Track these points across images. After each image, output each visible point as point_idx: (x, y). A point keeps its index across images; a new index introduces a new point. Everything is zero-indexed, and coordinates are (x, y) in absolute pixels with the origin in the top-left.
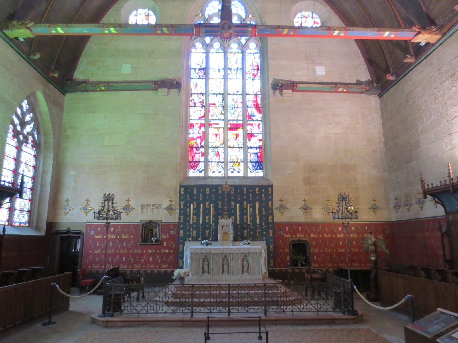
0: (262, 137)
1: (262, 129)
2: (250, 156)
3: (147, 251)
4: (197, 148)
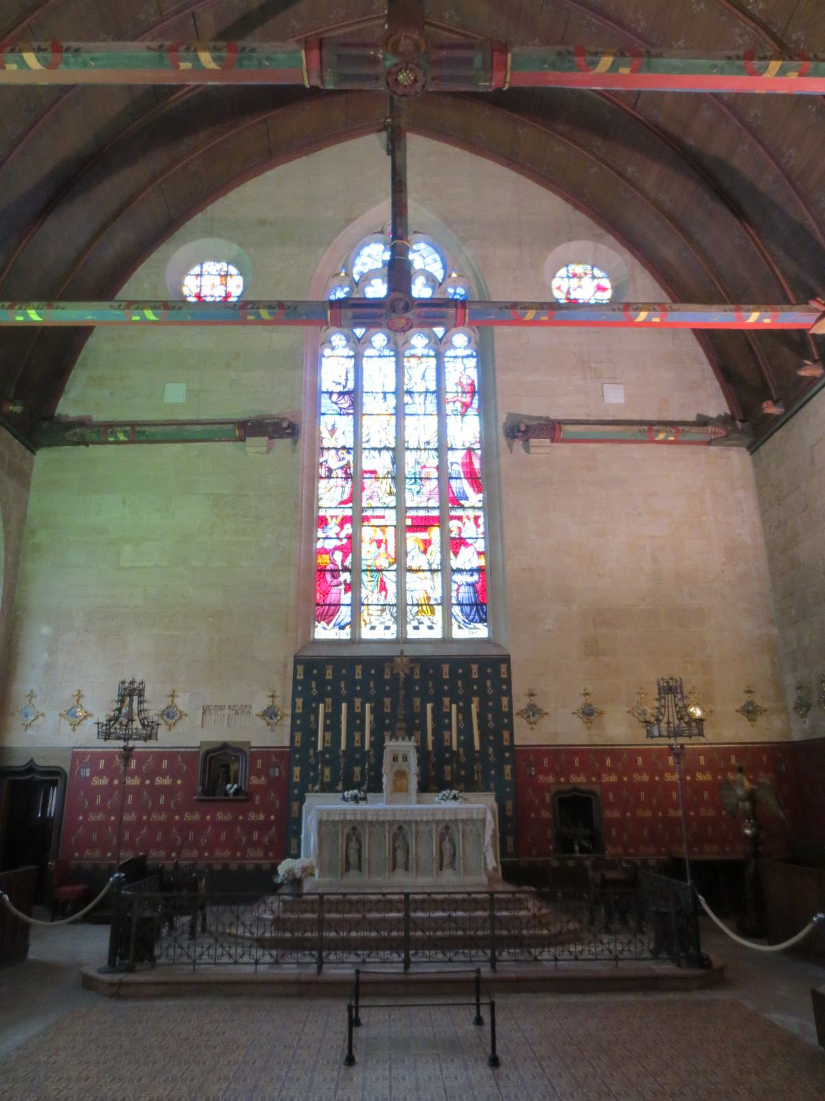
0: (485, 547)
1: (485, 527)
2: (458, 590)
3: (214, 817)
4: (335, 573)
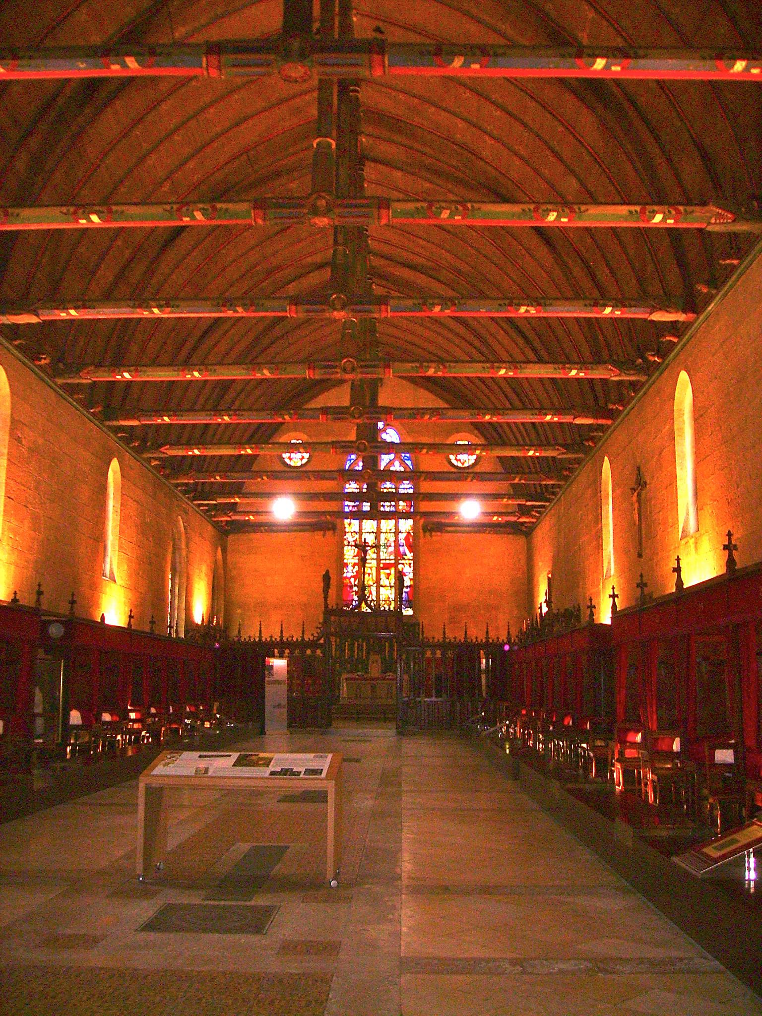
4: (351, 587)
